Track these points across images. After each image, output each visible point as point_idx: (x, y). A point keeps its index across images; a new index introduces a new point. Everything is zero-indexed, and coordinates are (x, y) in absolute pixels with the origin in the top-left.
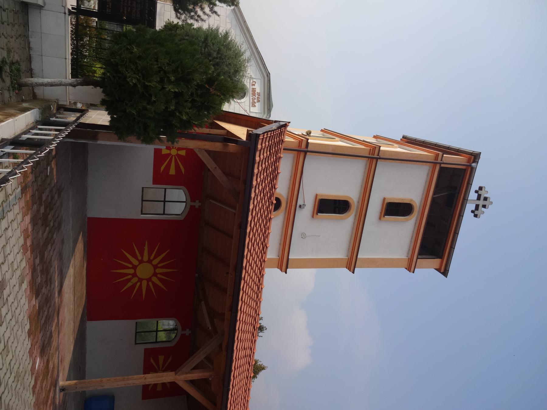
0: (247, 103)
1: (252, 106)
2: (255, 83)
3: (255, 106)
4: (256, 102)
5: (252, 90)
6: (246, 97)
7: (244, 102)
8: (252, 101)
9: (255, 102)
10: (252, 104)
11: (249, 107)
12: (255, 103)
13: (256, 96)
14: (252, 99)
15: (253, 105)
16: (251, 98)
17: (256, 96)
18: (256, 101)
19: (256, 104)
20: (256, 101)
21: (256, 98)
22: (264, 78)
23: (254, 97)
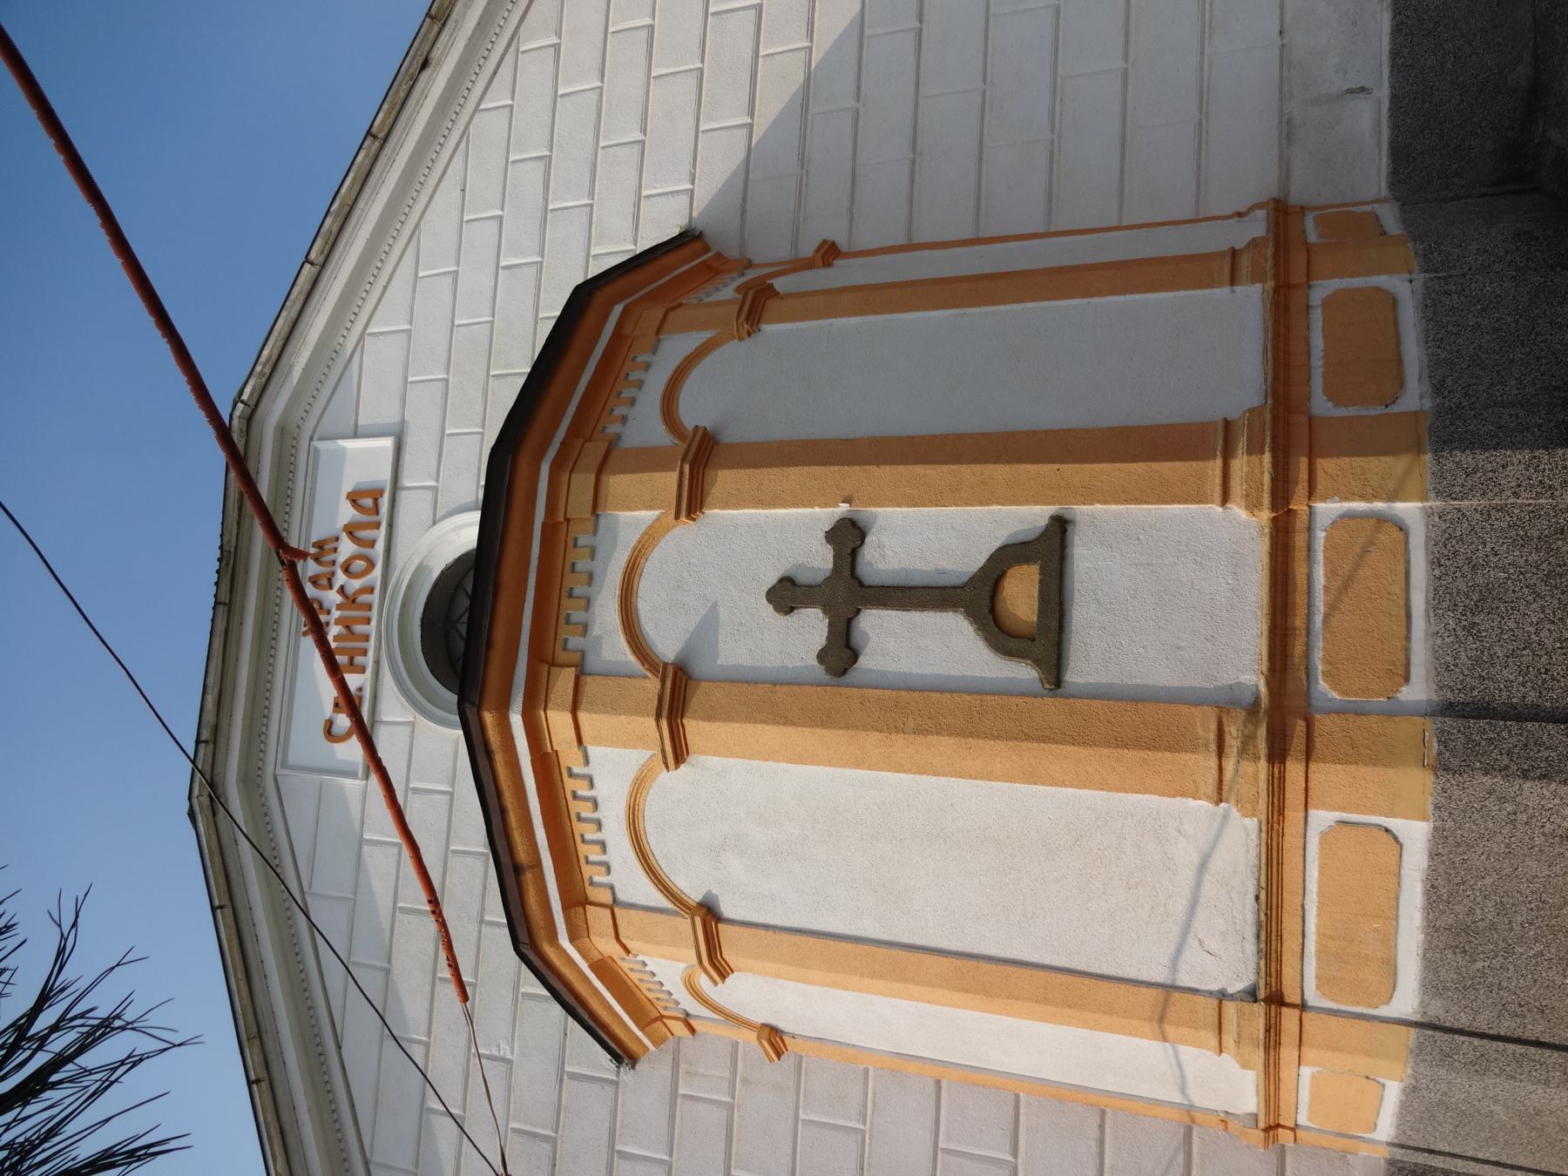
0: (412, 508)
1: (376, 494)
2: (329, 724)
3: (354, 498)
4: (344, 537)
5: (365, 652)
6: (421, 569)
7: (434, 523)
8: (372, 544)
9: (351, 534)
10: (377, 511)
11: (406, 482)
12: (351, 530)
13: (342, 590)
14: (371, 565)
15: (368, 502)
16: (378, 572)
17: (339, 599)
18: (347, 548)
19: (347, 513)
20: (347, 548)
21: (341, 578)
22: (252, 780)
23: (356, 584)
